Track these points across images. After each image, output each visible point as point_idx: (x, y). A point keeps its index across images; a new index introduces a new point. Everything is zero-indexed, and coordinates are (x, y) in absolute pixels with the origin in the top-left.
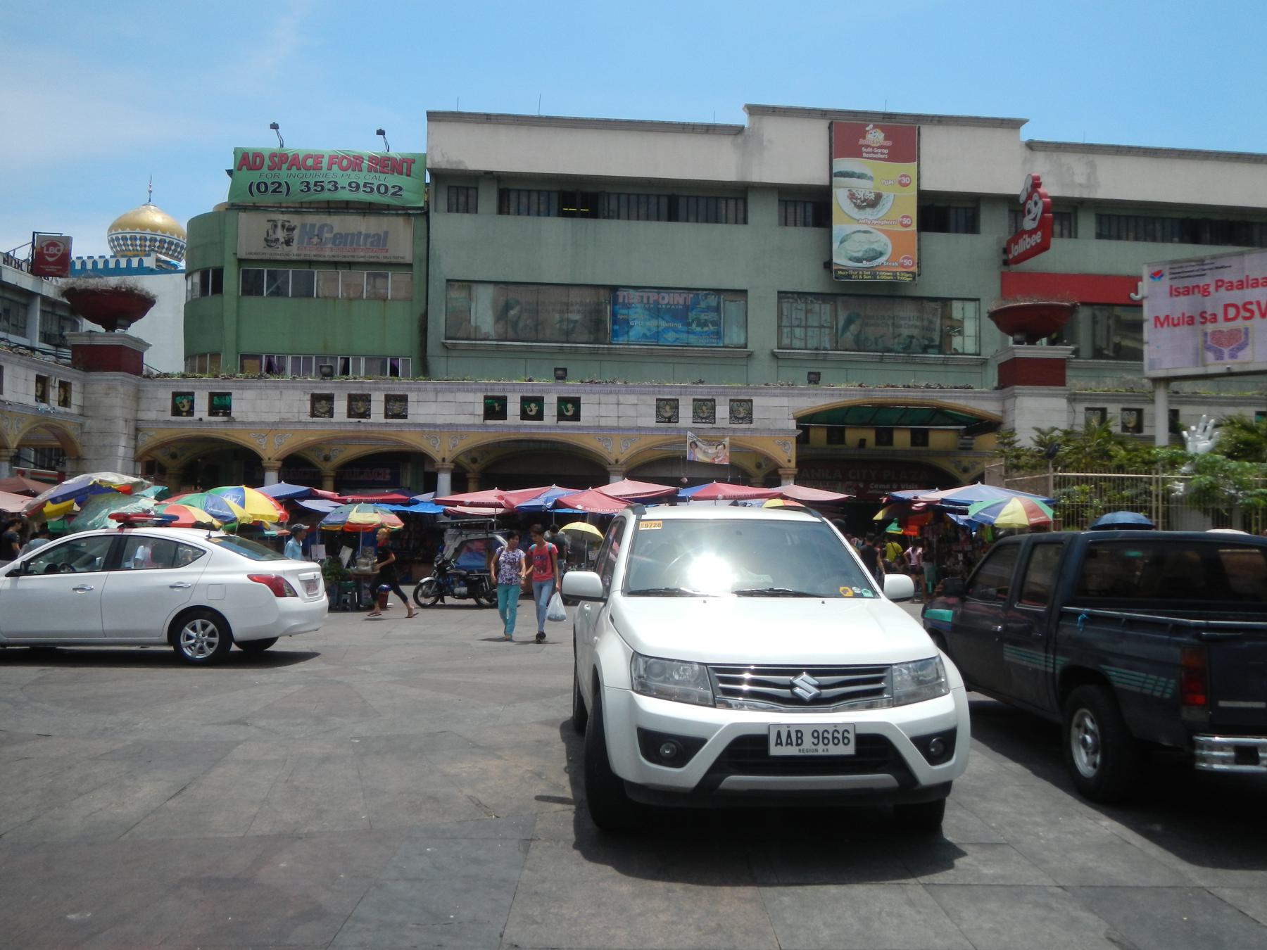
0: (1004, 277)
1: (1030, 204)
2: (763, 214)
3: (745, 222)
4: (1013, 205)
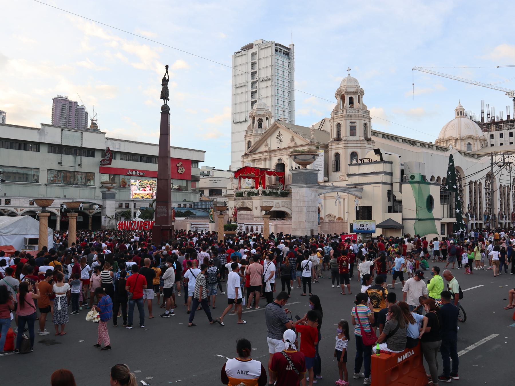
0: (100, 167)
1: (107, 154)
2: (44, 149)
3: (39, 151)
4: (103, 151)
